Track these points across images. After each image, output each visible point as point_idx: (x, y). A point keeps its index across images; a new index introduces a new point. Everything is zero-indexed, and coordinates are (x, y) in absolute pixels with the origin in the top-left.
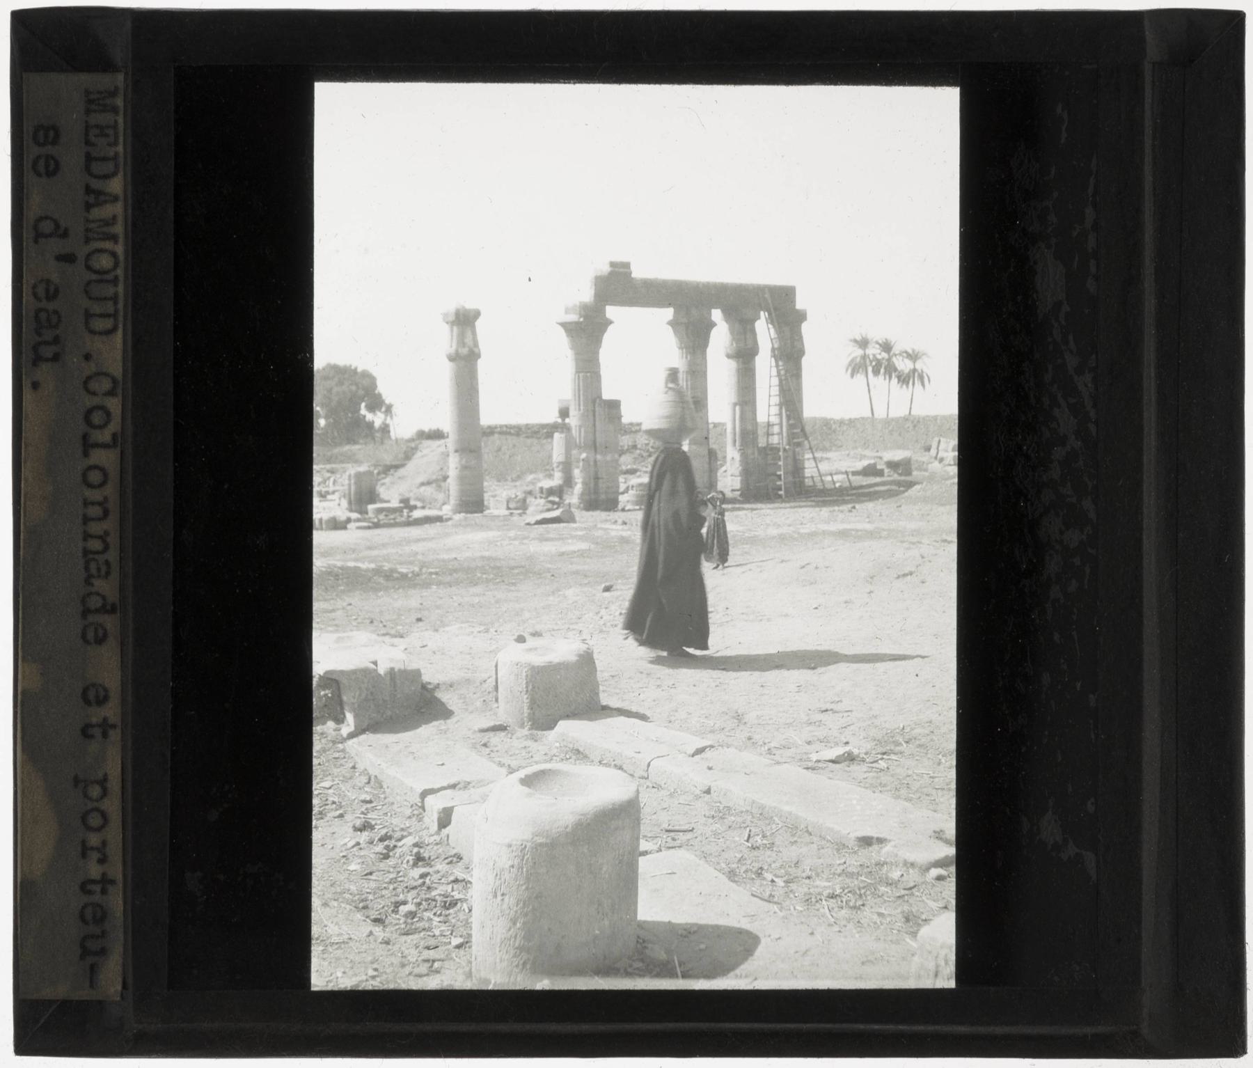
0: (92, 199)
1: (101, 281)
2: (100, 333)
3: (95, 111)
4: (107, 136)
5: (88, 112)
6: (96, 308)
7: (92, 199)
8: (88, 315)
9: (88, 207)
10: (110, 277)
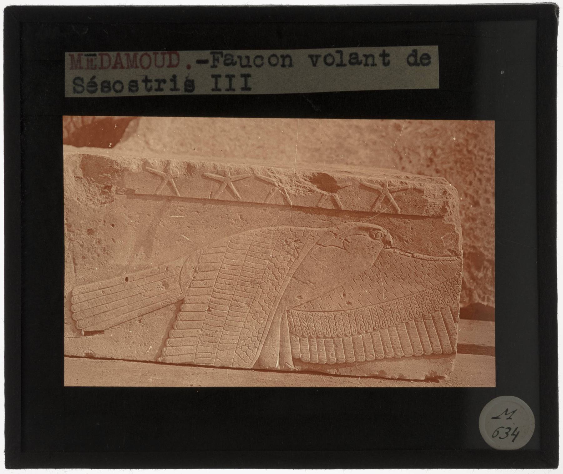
0: (119, 66)
1: (156, 60)
2: (179, 60)
3: (80, 64)
4: (92, 60)
5: (81, 68)
6: (167, 63)
7: (119, 66)
8: (170, 66)
9: (122, 67)
10: (153, 57)
